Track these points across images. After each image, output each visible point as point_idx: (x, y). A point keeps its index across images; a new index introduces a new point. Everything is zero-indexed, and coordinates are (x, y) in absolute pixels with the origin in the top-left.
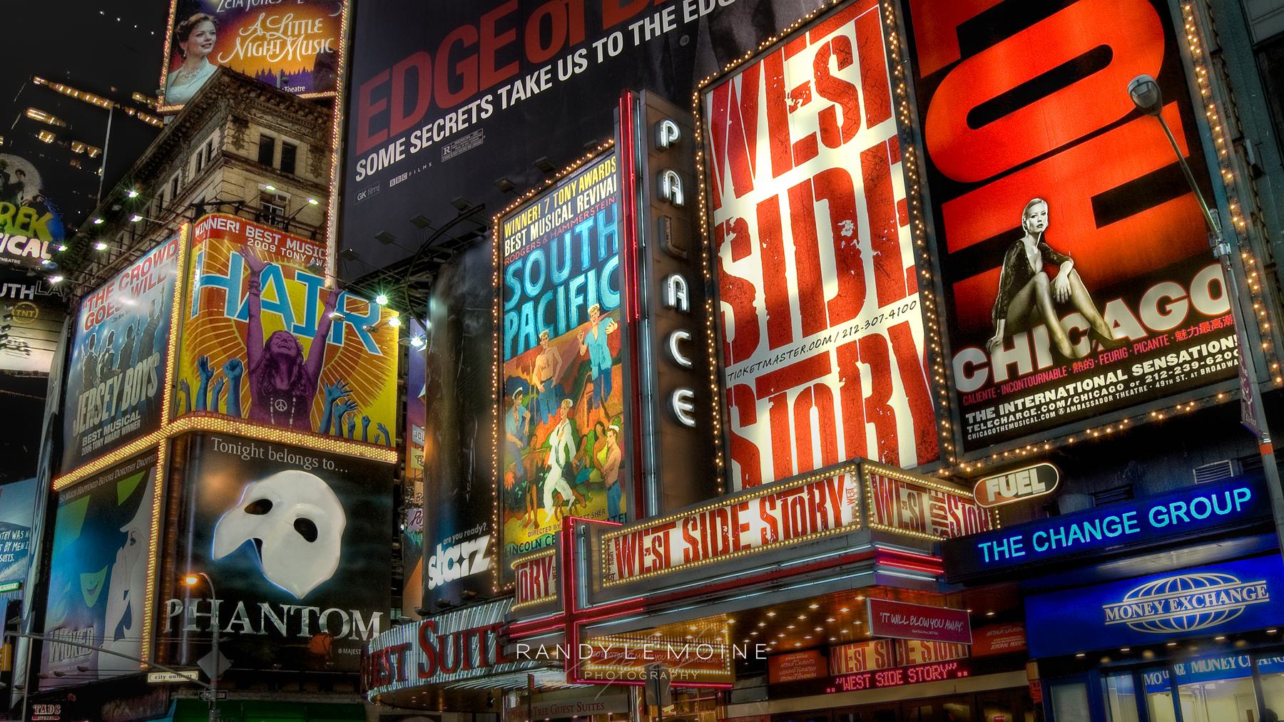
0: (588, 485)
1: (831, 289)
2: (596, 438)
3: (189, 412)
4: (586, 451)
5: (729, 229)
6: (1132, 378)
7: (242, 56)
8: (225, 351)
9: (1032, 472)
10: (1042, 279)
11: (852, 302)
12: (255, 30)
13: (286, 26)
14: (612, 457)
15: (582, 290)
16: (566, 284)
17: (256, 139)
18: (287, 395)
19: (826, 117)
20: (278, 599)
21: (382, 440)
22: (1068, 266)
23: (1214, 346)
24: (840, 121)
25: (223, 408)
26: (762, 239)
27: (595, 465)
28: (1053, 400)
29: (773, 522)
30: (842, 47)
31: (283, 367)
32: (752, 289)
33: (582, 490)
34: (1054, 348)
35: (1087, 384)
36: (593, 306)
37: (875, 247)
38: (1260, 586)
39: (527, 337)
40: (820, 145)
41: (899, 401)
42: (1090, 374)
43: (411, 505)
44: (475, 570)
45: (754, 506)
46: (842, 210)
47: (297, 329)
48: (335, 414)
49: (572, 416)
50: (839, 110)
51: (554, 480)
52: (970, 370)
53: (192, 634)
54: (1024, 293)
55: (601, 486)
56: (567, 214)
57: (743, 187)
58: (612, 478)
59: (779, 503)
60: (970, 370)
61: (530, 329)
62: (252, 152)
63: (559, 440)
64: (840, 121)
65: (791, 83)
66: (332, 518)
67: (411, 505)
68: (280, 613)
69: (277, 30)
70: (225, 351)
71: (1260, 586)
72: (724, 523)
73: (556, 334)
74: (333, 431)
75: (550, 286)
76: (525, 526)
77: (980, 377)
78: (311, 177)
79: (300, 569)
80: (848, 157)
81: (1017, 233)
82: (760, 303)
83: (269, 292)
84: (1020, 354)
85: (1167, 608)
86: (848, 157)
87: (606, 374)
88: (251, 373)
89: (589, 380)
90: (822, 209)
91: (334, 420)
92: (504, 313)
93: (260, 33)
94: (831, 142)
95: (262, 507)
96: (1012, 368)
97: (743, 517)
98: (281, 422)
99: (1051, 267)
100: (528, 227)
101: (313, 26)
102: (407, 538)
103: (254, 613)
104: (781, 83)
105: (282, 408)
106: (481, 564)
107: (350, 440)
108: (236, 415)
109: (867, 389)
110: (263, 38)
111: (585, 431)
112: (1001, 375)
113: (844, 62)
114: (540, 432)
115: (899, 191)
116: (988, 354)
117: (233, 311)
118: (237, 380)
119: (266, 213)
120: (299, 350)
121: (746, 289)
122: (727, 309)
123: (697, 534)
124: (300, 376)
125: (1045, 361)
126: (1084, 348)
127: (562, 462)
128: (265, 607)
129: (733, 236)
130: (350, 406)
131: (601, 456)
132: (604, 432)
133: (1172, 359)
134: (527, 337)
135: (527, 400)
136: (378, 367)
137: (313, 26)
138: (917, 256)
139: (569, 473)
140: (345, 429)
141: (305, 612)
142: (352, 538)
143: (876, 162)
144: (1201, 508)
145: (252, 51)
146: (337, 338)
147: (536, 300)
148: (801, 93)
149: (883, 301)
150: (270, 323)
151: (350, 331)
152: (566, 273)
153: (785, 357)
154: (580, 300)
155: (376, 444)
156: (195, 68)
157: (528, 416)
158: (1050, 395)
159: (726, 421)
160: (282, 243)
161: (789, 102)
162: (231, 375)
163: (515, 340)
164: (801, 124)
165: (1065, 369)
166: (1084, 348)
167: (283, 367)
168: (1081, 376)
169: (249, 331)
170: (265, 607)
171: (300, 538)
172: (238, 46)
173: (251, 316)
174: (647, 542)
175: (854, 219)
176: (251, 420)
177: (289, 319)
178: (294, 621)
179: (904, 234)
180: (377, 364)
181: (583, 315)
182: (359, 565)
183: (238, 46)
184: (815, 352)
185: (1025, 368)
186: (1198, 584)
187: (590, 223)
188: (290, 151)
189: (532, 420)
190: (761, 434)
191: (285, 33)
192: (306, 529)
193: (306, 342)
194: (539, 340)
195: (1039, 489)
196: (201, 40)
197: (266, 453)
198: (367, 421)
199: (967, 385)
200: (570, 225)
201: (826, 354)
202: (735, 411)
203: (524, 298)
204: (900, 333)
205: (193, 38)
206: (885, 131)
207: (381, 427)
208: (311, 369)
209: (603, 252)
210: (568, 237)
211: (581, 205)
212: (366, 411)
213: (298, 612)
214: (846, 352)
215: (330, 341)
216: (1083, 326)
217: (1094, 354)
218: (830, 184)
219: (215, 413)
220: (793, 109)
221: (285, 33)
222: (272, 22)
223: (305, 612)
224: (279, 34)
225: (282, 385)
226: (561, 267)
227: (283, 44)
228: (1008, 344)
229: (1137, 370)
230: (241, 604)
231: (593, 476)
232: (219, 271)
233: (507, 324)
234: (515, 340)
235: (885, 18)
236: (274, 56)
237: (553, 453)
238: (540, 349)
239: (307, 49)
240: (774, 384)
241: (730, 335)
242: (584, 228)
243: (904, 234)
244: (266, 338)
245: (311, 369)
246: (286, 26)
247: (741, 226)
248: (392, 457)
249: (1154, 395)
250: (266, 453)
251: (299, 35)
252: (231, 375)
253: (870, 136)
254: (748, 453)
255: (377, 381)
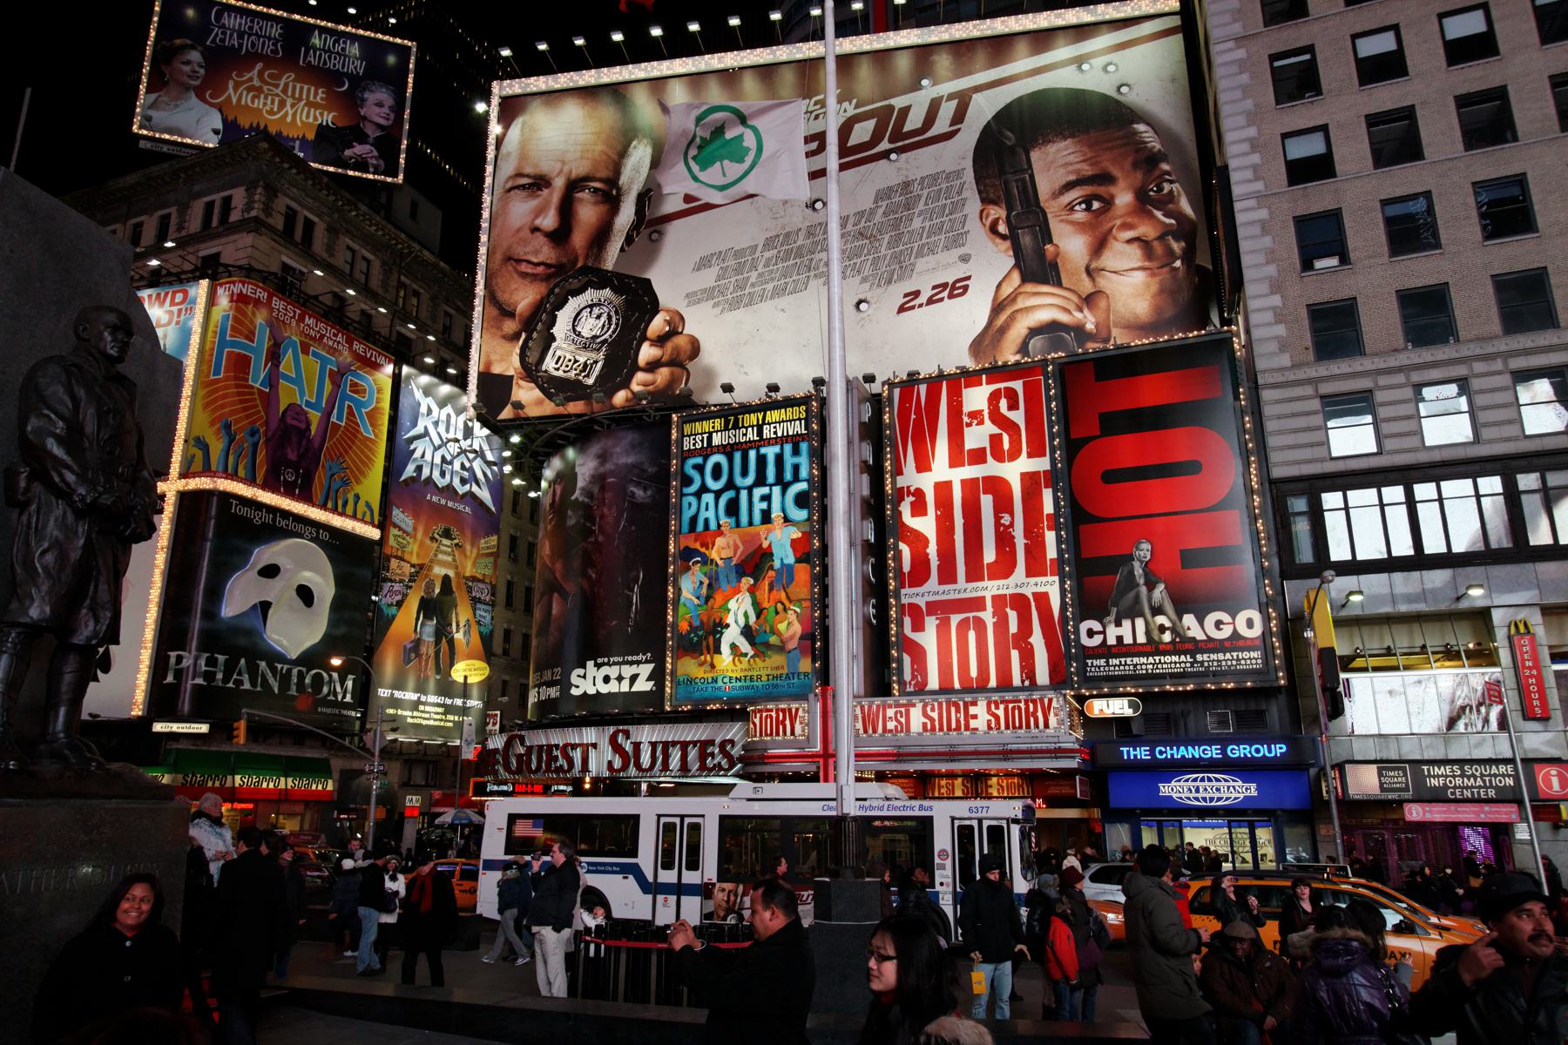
0: (767, 645)
1: (989, 555)
2: (777, 613)
3: (207, 471)
4: (766, 621)
5: (909, 493)
6: (1196, 661)
7: (234, 101)
8: (247, 417)
9: (1125, 701)
10: (1144, 590)
11: (1004, 567)
12: (251, 79)
13: (286, 85)
14: (791, 632)
15: (767, 498)
16: (750, 489)
17: (283, 210)
18: (295, 466)
19: (995, 440)
20: (274, 657)
21: (368, 518)
22: (1161, 587)
23: (1246, 655)
24: (1006, 446)
25: (241, 473)
26: (937, 508)
27: (774, 631)
28: (1146, 663)
29: (997, 718)
30: (1011, 395)
31: (294, 439)
32: (926, 541)
33: (761, 648)
34: (1148, 633)
35: (1168, 659)
36: (776, 513)
37: (1026, 537)
38: (1253, 786)
39: (706, 520)
40: (989, 458)
41: (1037, 640)
42: (1170, 653)
43: (387, 580)
44: (635, 688)
45: (982, 704)
46: (1003, 504)
47: (308, 404)
48: (334, 487)
49: (752, 590)
50: (1006, 438)
51: (732, 635)
52: (1091, 633)
53: (196, 687)
54: (1132, 594)
55: (781, 649)
56: (752, 435)
57: (923, 465)
58: (792, 645)
59: (1002, 707)
60: (1091, 633)
61: (711, 514)
62: (278, 222)
63: (739, 609)
64: (1006, 446)
65: (968, 407)
66: (325, 586)
67: (387, 580)
68: (274, 670)
69: (277, 86)
70: (247, 417)
71: (1253, 786)
72: (958, 711)
73: (738, 525)
74: (330, 505)
75: (730, 485)
76: (701, 665)
77: (1097, 640)
78: (325, 255)
79: (294, 633)
80: (1012, 472)
81: (1131, 558)
82: (932, 550)
83: (287, 364)
84: (1125, 631)
85: (1197, 791)
86: (1012, 472)
87: (788, 570)
88: (267, 442)
89: (771, 568)
90: (987, 501)
91: (332, 494)
92: (683, 495)
93: (256, 83)
94: (999, 456)
95: (271, 571)
96: (1120, 638)
97: (972, 710)
98: (289, 493)
99: (1151, 587)
100: (710, 434)
101: (316, 94)
102: (380, 610)
103: (253, 671)
104: (960, 404)
105: (291, 479)
106: (643, 685)
107: (342, 514)
108: (251, 481)
109: (1013, 628)
110: (259, 90)
111: (766, 605)
112: (1112, 641)
113: (1013, 406)
114: (719, 597)
115: (1048, 507)
116: (1104, 627)
117: (258, 377)
118: (255, 445)
119: (284, 284)
120: (308, 424)
121: (918, 540)
122: (905, 549)
123: (935, 715)
124: (307, 449)
125: (1141, 639)
126: (1167, 637)
127: (742, 622)
128: (263, 664)
129: (912, 499)
130: (346, 483)
131: (782, 627)
132: (785, 610)
133: (1221, 656)
134: (706, 520)
135: (705, 569)
136: (370, 449)
137: (316, 94)
138: (1060, 551)
139: (747, 632)
140: (340, 503)
141: (295, 671)
142: (338, 605)
143: (1031, 482)
144: (1257, 751)
145: (247, 99)
146: (340, 418)
147: (718, 494)
148: (976, 415)
149: (1030, 573)
150: (287, 395)
151: (351, 412)
152: (750, 480)
153: (950, 592)
154: (764, 505)
155: (362, 521)
156: (177, 99)
157: (706, 582)
158: (1144, 660)
159: (900, 625)
160: (301, 319)
161: (966, 419)
162: (251, 440)
163: (694, 520)
164: (976, 437)
165: (1153, 647)
166: (1167, 637)
167: (294, 439)
168: (1164, 653)
169: (269, 399)
170: (263, 664)
171: (299, 602)
172: (231, 90)
173: (271, 387)
174: (890, 712)
175: (1012, 515)
176: (264, 487)
177: (302, 394)
178: (285, 680)
179: (1050, 537)
180: (369, 444)
181: (766, 517)
182: (342, 630)
183: (231, 90)
184: (974, 595)
185: (1128, 640)
186: (1217, 780)
187: (777, 449)
188: (309, 226)
189: (710, 586)
190: (928, 639)
191: (285, 91)
192: (305, 594)
193: (315, 416)
194: (719, 526)
195: (1129, 712)
196: (187, 68)
197: (274, 520)
198: (357, 497)
199: (1086, 641)
200: (756, 445)
201: (983, 598)
202: (907, 621)
203: (704, 489)
204: (1042, 598)
205: (177, 65)
206: (1042, 464)
207: (368, 505)
208: (316, 444)
209: (788, 476)
210: (752, 454)
211: (767, 432)
212: (358, 489)
213: (289, 671)
214: (999, 600)
215: (334, 419)
216: (1168, 624)
217: (1173, 642)
218: (996, 486)
219: (233, 476)
220: (969, 425)
221: (285, 91)
222: (270, 76)
223: (295, 671)
224: (278, 91)
225: (292, 455)
226: (745, 473)
227: (282, 104)
228: (1118, 624)
229: (1199, 657)
230: (243, 661)
231: (773, 640)
232: (247, 338)
233: (685, 504)
234: (694, 520)
235: (1048, 389)
236: (271, 112)
237: (731, 614)
238: (719, 531)
239: (308, 116)
240: (941, 608)
241: (906, 567)
242: (771, 452)
243: (1050, 537)
244: (282, 409)
245: (316, 444)
246: (286, 85)
247: (919, 494)
248: (375, 534)
249: (1206, 674)
250: (274, 520)
251: (300, 99)
252: (251, 440)
253: (1025, 464)
254: (918, 653)
255: (368, 462)
